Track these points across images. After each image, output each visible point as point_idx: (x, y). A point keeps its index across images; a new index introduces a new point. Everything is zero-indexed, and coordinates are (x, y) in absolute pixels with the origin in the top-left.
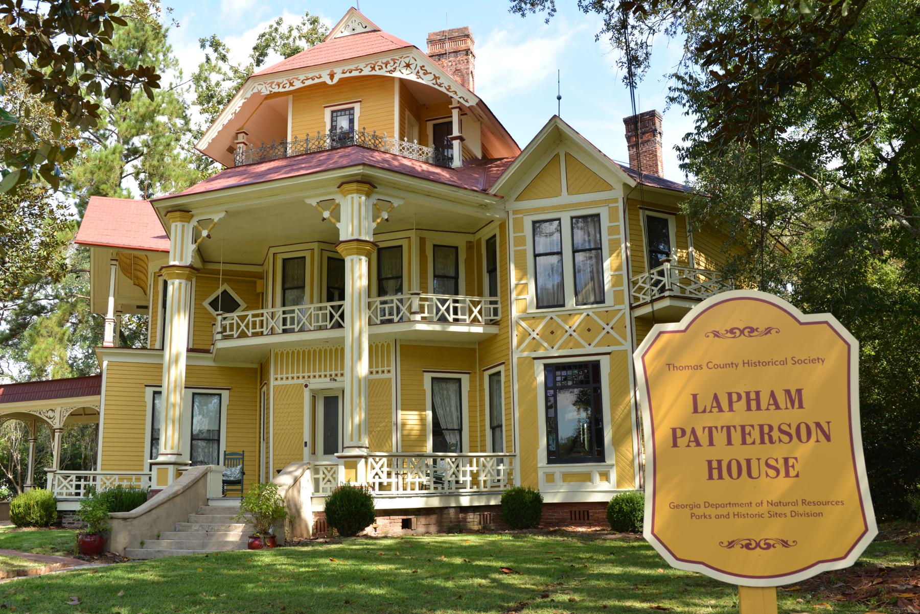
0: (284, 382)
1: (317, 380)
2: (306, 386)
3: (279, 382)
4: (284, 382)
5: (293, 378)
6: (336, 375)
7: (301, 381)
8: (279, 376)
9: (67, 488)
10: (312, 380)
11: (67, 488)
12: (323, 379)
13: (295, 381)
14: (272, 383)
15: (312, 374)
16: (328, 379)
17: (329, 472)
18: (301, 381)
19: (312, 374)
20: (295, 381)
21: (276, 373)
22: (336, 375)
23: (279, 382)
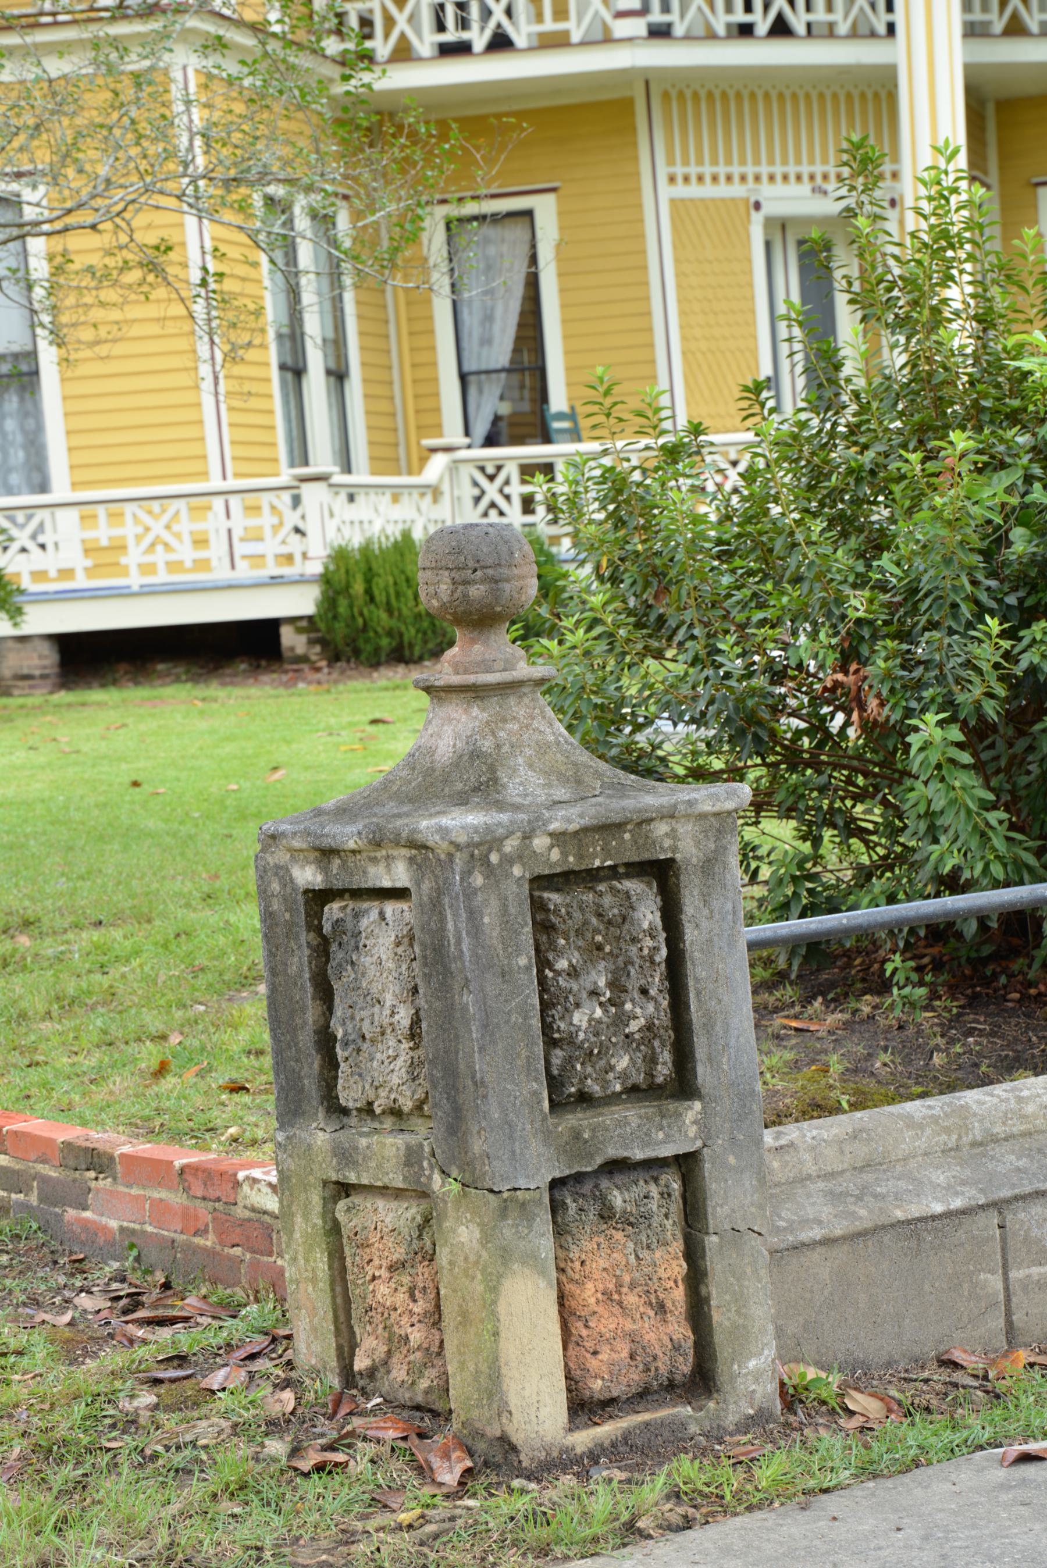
0: (694, 191)
1: (779, 189)
2: (757, 206)
3: (681, 191)
4: (694, 191)
5: (785, 178)
6: (825, 177)
7: (737, 190)
8: (679, 170)
9: (138, 538)
10: (766, 192)
11: (138, 538)
12: (793, 189)
13: (723, 190)
14: (666, 192)
15: (764, 170)
16: (806, 188)
17: (491, 478)
18: (737, 190)
19: (764, 170)
20: (723, 190)
21: (671, 161)
22: (825, 177)
23: (681, 191)
